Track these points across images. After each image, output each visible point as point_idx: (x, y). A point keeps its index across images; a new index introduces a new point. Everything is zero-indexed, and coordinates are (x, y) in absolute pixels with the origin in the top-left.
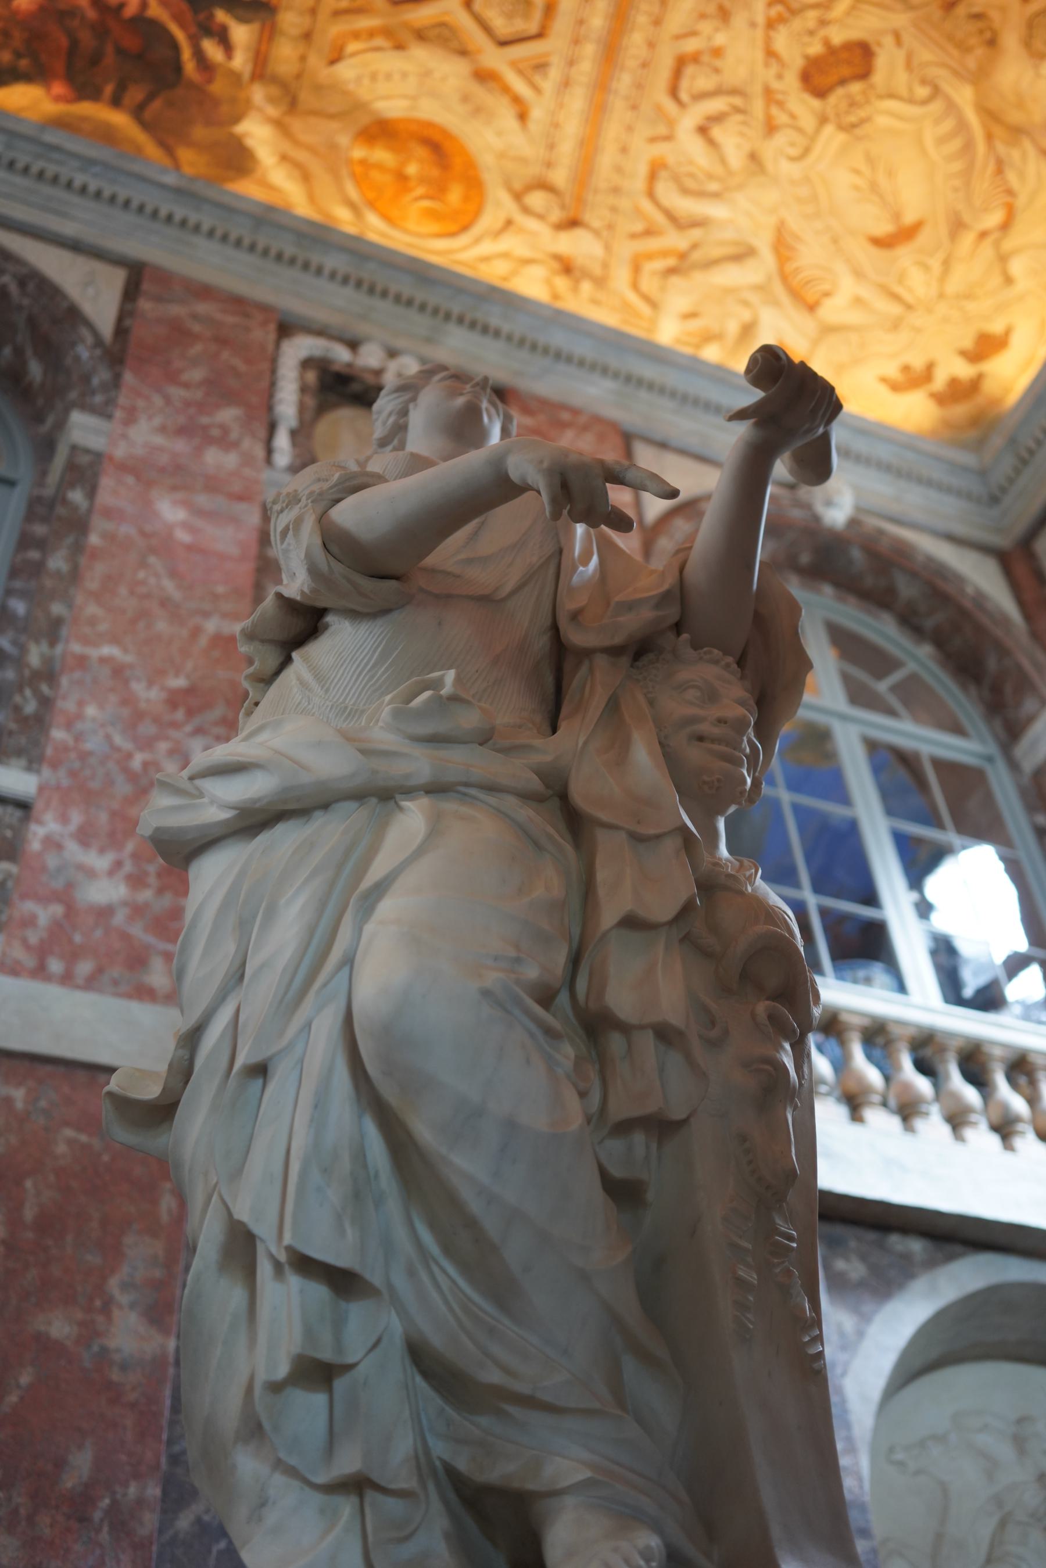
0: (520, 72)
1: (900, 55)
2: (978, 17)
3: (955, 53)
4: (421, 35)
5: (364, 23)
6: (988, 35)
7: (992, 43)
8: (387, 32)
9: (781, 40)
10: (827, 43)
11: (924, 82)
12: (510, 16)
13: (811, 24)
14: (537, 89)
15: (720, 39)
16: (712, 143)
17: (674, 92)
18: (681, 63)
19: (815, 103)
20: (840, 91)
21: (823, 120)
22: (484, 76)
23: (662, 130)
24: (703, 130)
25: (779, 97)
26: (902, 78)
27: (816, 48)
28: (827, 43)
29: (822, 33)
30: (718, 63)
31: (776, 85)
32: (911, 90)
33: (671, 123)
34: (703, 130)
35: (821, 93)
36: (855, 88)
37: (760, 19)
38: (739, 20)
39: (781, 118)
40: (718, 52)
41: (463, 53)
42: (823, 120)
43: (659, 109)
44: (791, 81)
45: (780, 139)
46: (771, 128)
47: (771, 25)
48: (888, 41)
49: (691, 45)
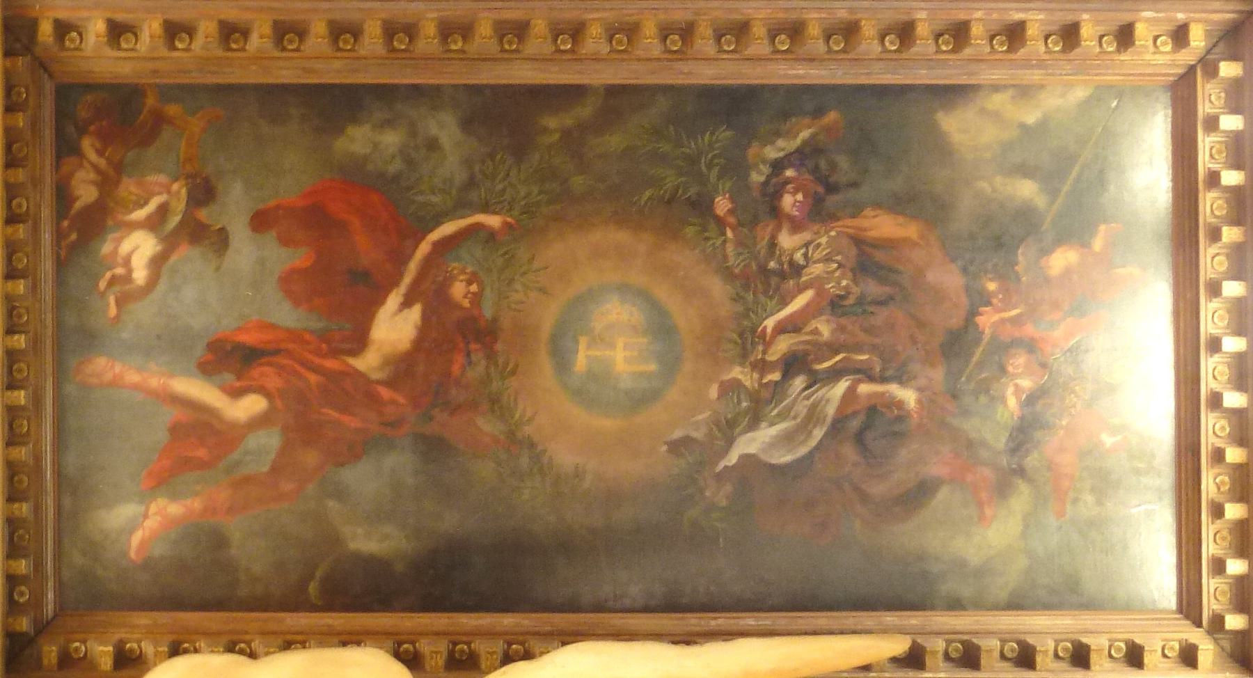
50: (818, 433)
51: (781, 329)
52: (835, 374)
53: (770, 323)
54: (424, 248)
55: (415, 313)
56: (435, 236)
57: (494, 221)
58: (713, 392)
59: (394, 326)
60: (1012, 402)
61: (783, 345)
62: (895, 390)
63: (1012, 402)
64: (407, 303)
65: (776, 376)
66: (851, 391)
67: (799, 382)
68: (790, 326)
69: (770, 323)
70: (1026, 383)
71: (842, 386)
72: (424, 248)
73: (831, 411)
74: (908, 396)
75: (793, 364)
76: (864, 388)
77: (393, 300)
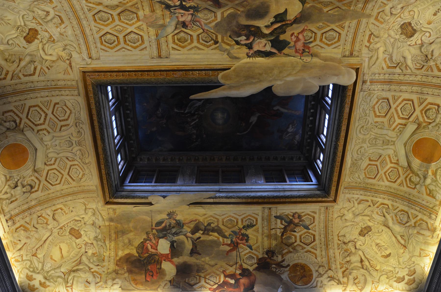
0: (93, 8)
1: (21, 46)
2: (13, 62)
3: (11, 53)
4: (117, 6)
5: (130, 4)
6: (8, 60)
7: (6, 60)
8: (125, 4)
9: (46, 34)
10: (38, 39)
11: (12, 44)
12: (102, 16)
13: (43, 40)
14: (86, 6)
15: (59, 29)
16: (44, 11)
17: (60, 17)
18: (62, 22)
19: (30, 28)
20: (27, 32)
21: (25, 25)
22: (100, 4)
23: (56, 9)
24: (48, 12)
25: (38, 25)
26: (17, 41)
27: (39, 37)
28: (38, 39)
29: (40, 40)
30: (56, 25)
31: (41, 26)
32: (13, 41)
33: (55, 11)
34: (48, 12)
35: (30, 30)
36: (25, 35)
37: (53, 36)
38: (57, 35)
39: (34, 21)
40: (57, 27)
41: (107, 6)
42: (25, 25)
43: (60, 12)
44: (38, 28)
45: (31, 18)
46: (34, 18)
47: (51, 36)
48: (26, 46)
49: (63, 26)
50: (189, 105)
51: (196, 120)
52: (188, 113)
53: (197, 120)
54: (249, 130)
55: (250, 121)
56: (247, 132)
57: (238, 134)
58: (205, 110)
59: (254, 119)
60: (160, 110)
61: (195, 117)
62: (178, 111)
63: (160, 110)
64: (252, 122)
65: (196, 113)
66: (185, 111)
67: (193, 112)
68: (194, 120)
69: (197, 120)
70: (158, 112)
71: (186, 112)
72: (249, 130)
73: (188, 108)
74: (176, 110)
75: (194, 115)
76: (183, 111)
77: (254, 123)
